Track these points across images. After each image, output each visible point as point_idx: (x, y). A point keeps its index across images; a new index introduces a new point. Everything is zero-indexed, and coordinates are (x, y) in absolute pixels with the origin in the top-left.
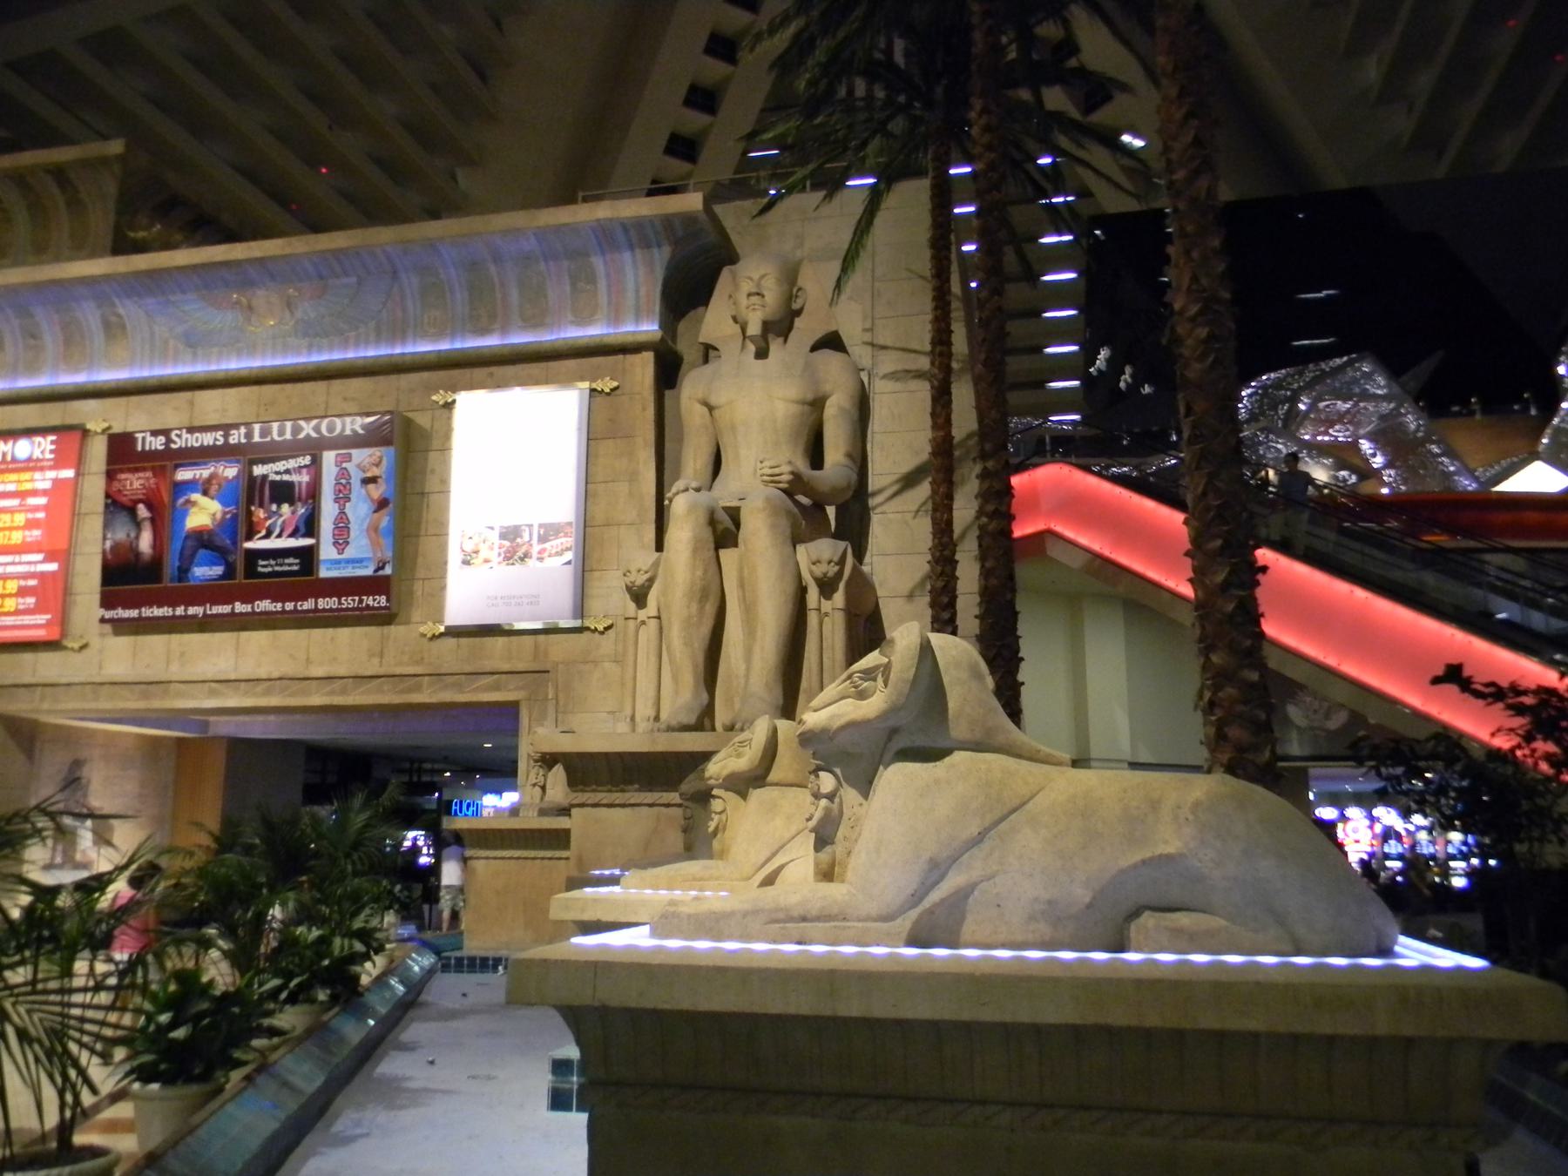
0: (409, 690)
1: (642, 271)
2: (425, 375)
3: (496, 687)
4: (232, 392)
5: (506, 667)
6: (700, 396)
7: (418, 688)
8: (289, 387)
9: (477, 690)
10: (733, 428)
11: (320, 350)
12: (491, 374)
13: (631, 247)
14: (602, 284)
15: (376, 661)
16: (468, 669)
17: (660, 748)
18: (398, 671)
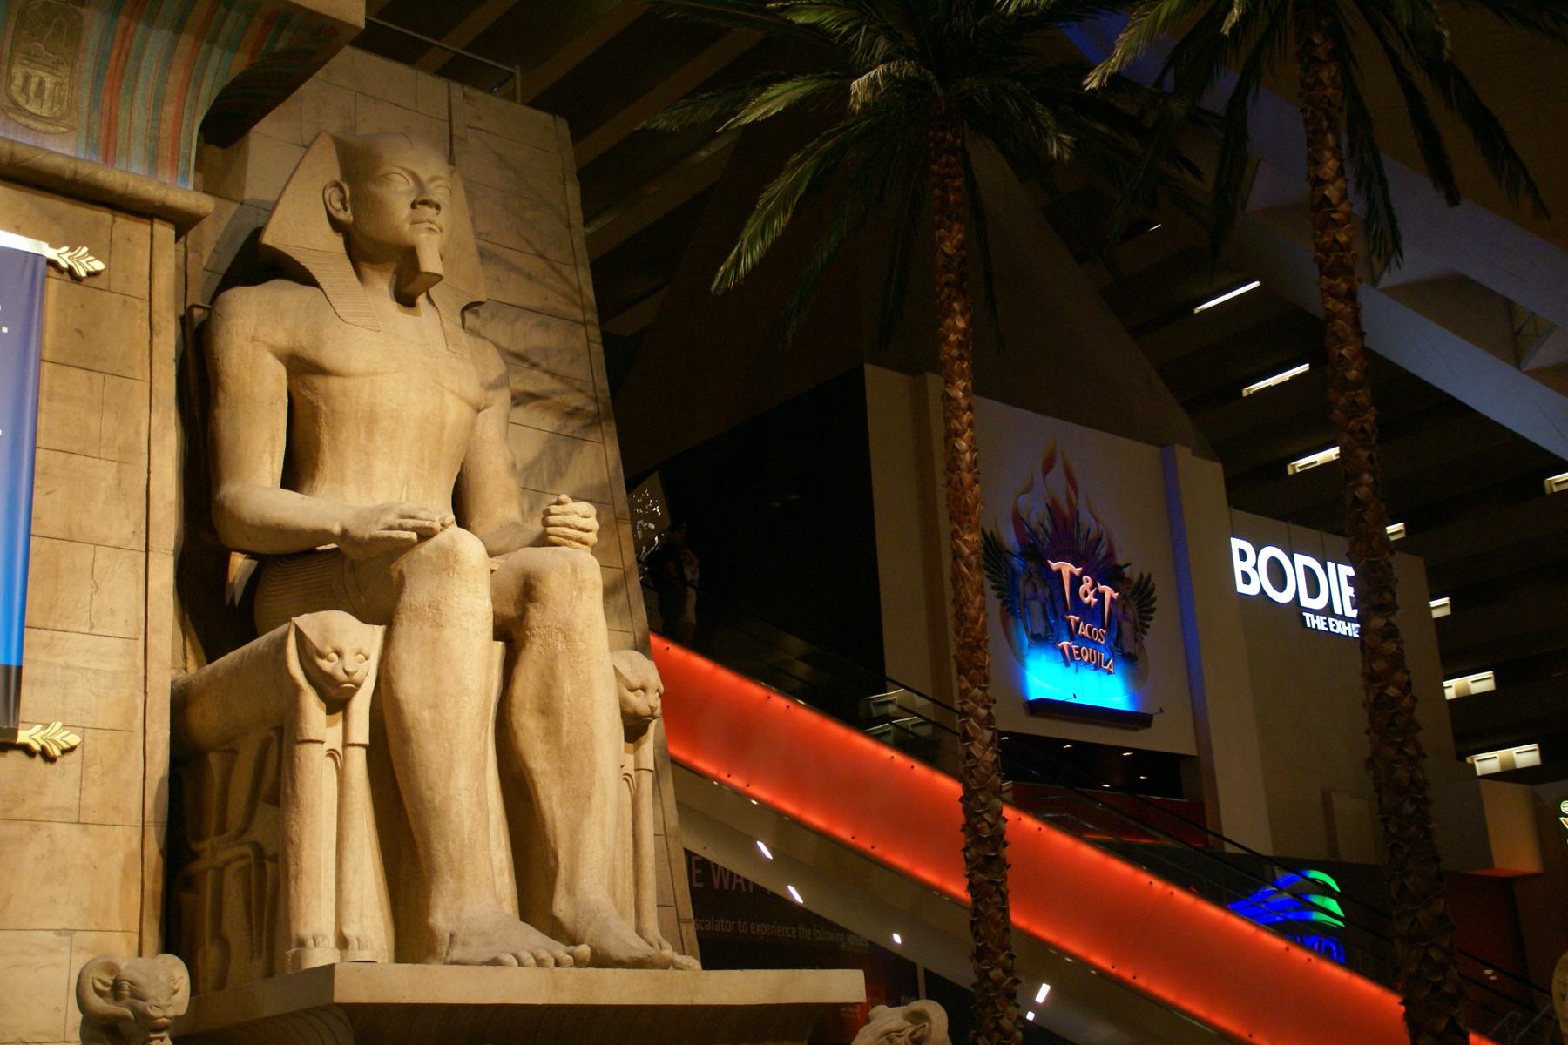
1: (175, 79)
6: (283, 340)
10: (372, 420)
13: (179, 28)
17: (566, 998)
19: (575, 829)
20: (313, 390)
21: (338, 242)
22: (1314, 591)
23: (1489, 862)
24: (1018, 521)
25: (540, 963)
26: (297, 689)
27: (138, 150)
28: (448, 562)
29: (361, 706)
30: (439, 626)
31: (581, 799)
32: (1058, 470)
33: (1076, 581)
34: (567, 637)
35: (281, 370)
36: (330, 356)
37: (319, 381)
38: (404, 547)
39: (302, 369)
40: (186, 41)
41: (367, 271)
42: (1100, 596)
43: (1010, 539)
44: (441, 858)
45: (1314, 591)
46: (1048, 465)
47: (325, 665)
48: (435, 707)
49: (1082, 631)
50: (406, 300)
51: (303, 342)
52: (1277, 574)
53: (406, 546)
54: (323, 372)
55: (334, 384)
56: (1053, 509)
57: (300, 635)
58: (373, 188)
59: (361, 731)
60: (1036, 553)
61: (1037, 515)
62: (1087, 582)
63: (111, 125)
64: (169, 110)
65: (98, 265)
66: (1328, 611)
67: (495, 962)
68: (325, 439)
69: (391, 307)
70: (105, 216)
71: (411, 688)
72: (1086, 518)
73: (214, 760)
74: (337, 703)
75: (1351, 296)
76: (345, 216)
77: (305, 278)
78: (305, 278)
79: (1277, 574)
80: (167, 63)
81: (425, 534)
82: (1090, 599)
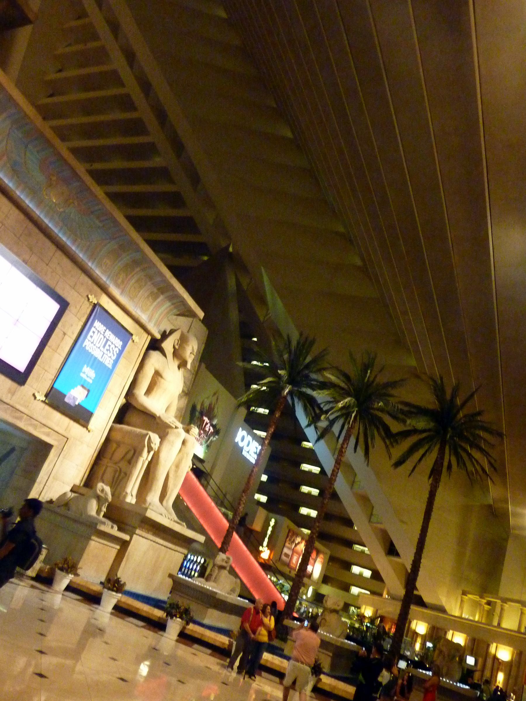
0: (17, 418)
1: (166, 311)
2: (90, 282)
3: (48, 435)
4: (15, 212)
5: (56, 429)
6: (157, 368)
7: (20, 419)
8: (41, 236)
9: (39, 432)
11: (65, 234)
12: (108, 302)
14: (155, 303)
15: (10, 395)
16: (44, 422)
18: (18, 407)
19: (172, 490)
20: (158, 379)
21: (172, 350)
22: (248, 445)
23: (252, 526)
24: (202, 404)
25: (169, 518)
26: (144, 446)
27: (153, 322)
28: (178, 435)
29: (152, 453)
30: (172, 446)
31: (175, 485)
32: (216, 396)
33: (207, 424)
34: (187, 456)
35: (153, 372)
36: (164, 375)
37: (160, 378)
38: (170, 427)
39: (157, 374)
40: (172, 306)
41: (175, 359)
42: (209, 429)
43: (198, 408)
44: (153, 489)
45: (248, 445)
46: (215, 394)
47: (152, 445)
48: (165, 461)
49: (202, 436)
50: (179, 368)
51: (161, 370)
52: (243, 439)
53: (172, 428)
54: (161, 377)
55: (162, 380)
56: (210, 405)
57: (150, 437)
58: (185, 346)
59: (149, 459)
60: (202, 414)
61: (206, 404)
62: (209, 424)
63: (152, 315)
64: (161, 317)
65: (138, 341)
66: (248, 452)
67: (161, 515)
68: (155, 389)
69: (177, 368)
70: (142, 331)
71: (163, 456)
72: (216, 409)
73: (115, 445)
74: (149, 452)
75: (338, 469)
76: (177, 347)
77: (164, 355)
78: (164, 355)
79: (243, 439)
80: (166, 309)
81: (176, 428)
82: (207, 429)
